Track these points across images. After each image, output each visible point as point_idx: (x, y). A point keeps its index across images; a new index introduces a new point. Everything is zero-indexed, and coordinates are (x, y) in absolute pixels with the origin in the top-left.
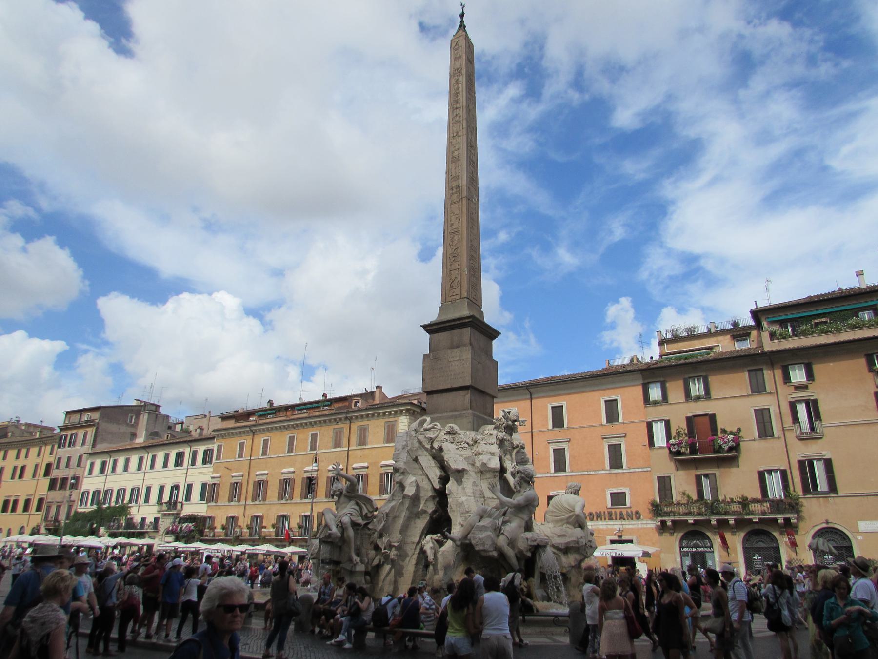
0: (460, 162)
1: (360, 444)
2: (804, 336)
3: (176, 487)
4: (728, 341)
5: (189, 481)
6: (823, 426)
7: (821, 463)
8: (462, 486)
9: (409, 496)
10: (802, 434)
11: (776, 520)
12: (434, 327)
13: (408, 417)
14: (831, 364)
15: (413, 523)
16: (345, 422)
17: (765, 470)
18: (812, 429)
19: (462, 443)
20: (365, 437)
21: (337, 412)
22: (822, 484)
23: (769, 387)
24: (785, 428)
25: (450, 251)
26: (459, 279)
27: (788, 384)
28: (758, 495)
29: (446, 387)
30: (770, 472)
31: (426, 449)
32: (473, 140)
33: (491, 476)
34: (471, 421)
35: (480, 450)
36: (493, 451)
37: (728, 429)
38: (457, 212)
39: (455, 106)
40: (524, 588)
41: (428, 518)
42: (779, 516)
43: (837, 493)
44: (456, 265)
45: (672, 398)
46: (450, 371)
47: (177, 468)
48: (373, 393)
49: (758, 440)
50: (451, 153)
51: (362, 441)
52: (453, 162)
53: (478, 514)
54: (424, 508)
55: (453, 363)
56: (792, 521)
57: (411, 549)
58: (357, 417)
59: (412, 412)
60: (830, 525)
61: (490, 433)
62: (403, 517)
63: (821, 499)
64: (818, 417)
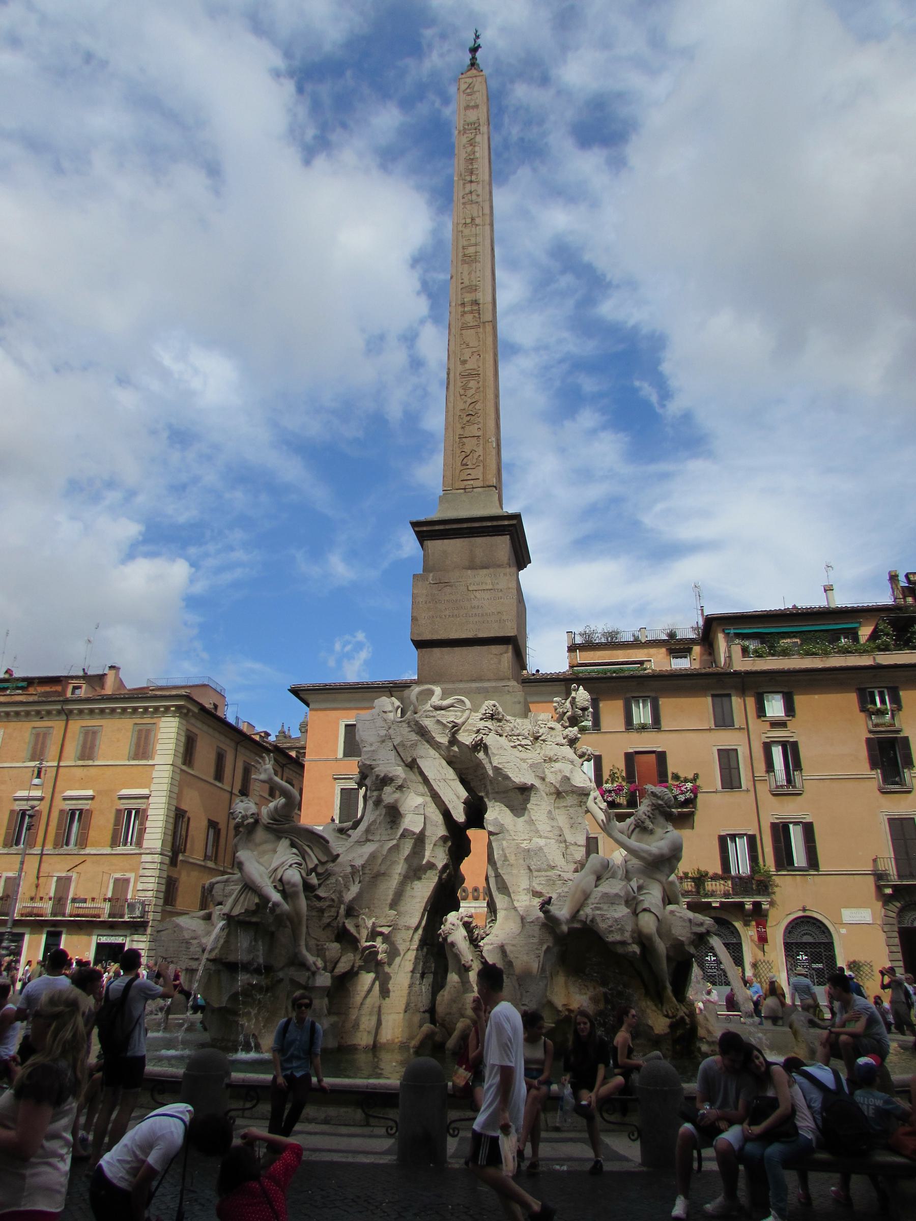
0: (478, 265)
1: (82, 758)
2: (785, 656)
4: (660, 656)
6: (804, 778)
7: (799, 828)
8: (526, 817)
9: (414, 834)
10: (777, 787)
11: (742, 904)
12: (437, 528)
13: (177, 719)
14: (816, 697)
15: (409, 888)
16: (57, 718)
17: (728, 834)
18: (789, 781)
19: (520, 738)
20: (92, 747)
21: (41, 699)
22: (799, 857)
23: (738, 720)
25: (461, 405)
27: (763, 719)
28: (719, 871)
30: (733, 837)
31: (436, 745)
33: (575, 802)
34: (522, 700)
35: (551, 754)
37: (682, 775)
39: (468, 178)
40: (686, 1017)
41: (436, 879)
42: (748, 900)
43: (818, 870)
44: (473, 430)
45: (605, 725)
48: (101, 678)
49: (721, 792)
50: (461, 249)
51: (87, 752)
52: (464, 262)
53: (595, 872)
54: (432, 860)
55: (477, 594)
56: (763, 906)
57: (404, 941)
58: (81, 711)
59: (185, 711)
60: (808, 913)
61: (550, 726)
62: (397, 877)
63: (798, 877)
64: (798, 766)
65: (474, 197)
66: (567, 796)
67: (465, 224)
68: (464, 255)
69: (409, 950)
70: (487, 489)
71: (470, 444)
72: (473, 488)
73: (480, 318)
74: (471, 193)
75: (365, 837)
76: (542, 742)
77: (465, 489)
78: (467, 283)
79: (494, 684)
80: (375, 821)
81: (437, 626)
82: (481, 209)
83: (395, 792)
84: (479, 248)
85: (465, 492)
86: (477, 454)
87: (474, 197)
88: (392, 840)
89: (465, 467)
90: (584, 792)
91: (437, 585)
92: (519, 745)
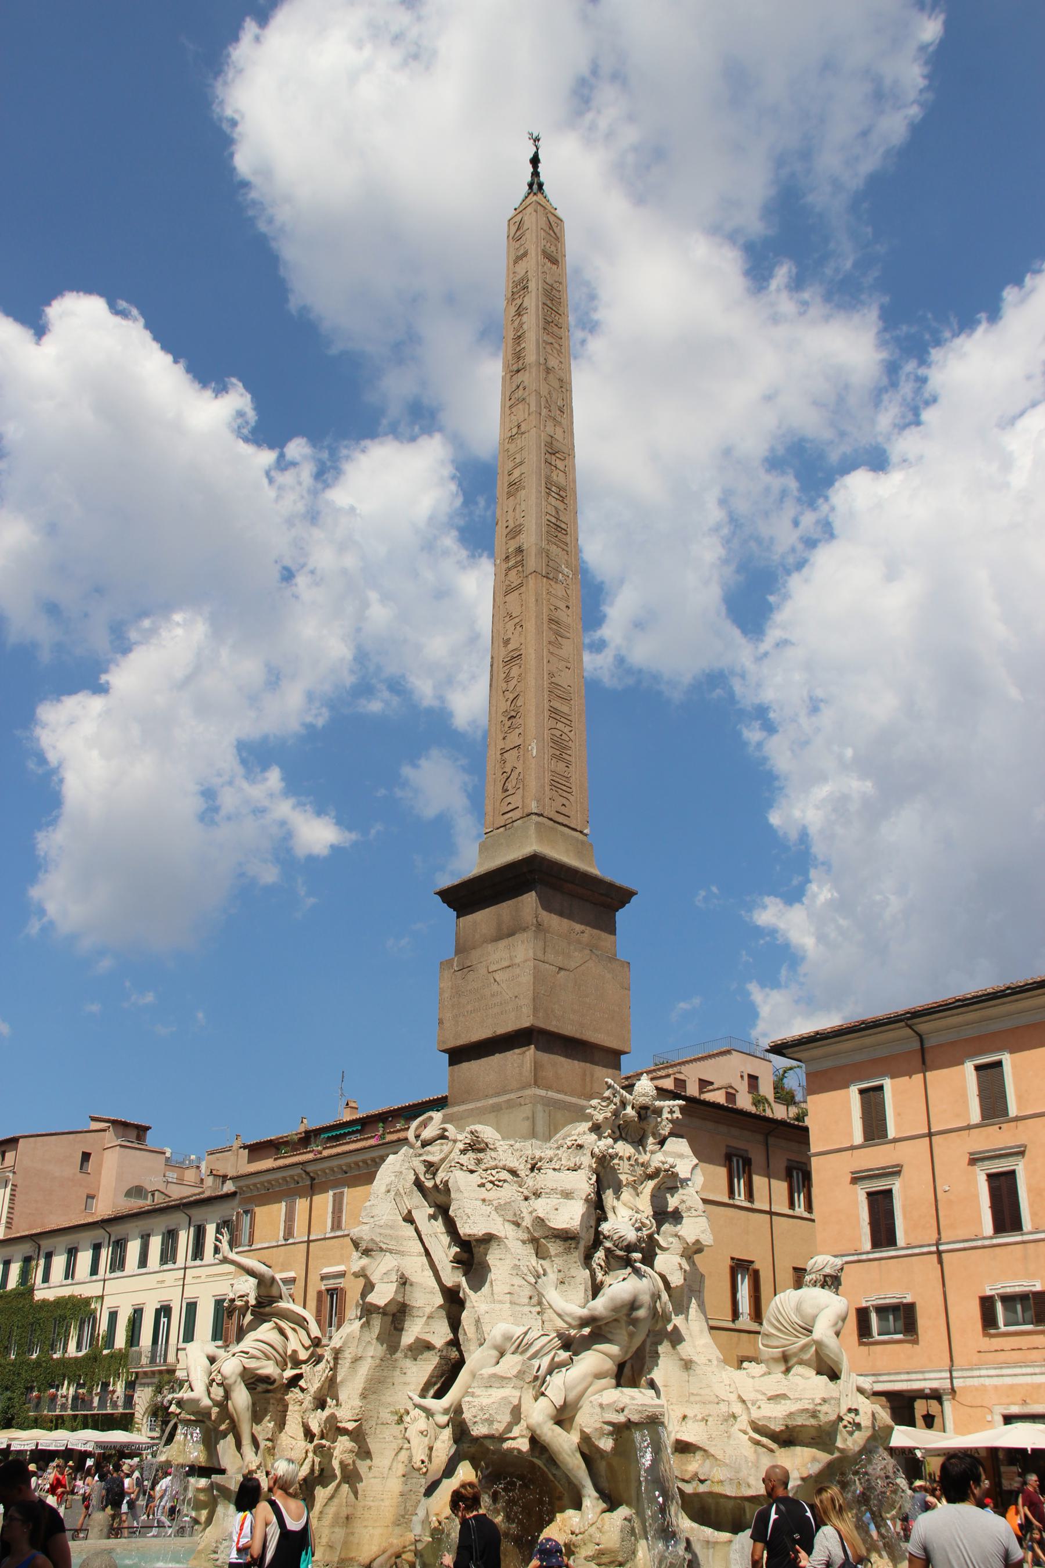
3: (164, 1311)
5: (190, 1293)
9: (379, 1307)
19: (494, 1172)
25: (504, 706)
32: (559, 435)
33: (561, 1250)
36: (568, 1187)
39: (515, 367)
44: (514, 739)
46: (493, 995)
47: (165, 1267)
65: (520, 392)
69: (401, 1449)
70: (526, 818)
77: (505, 826)
86: (517, 771)
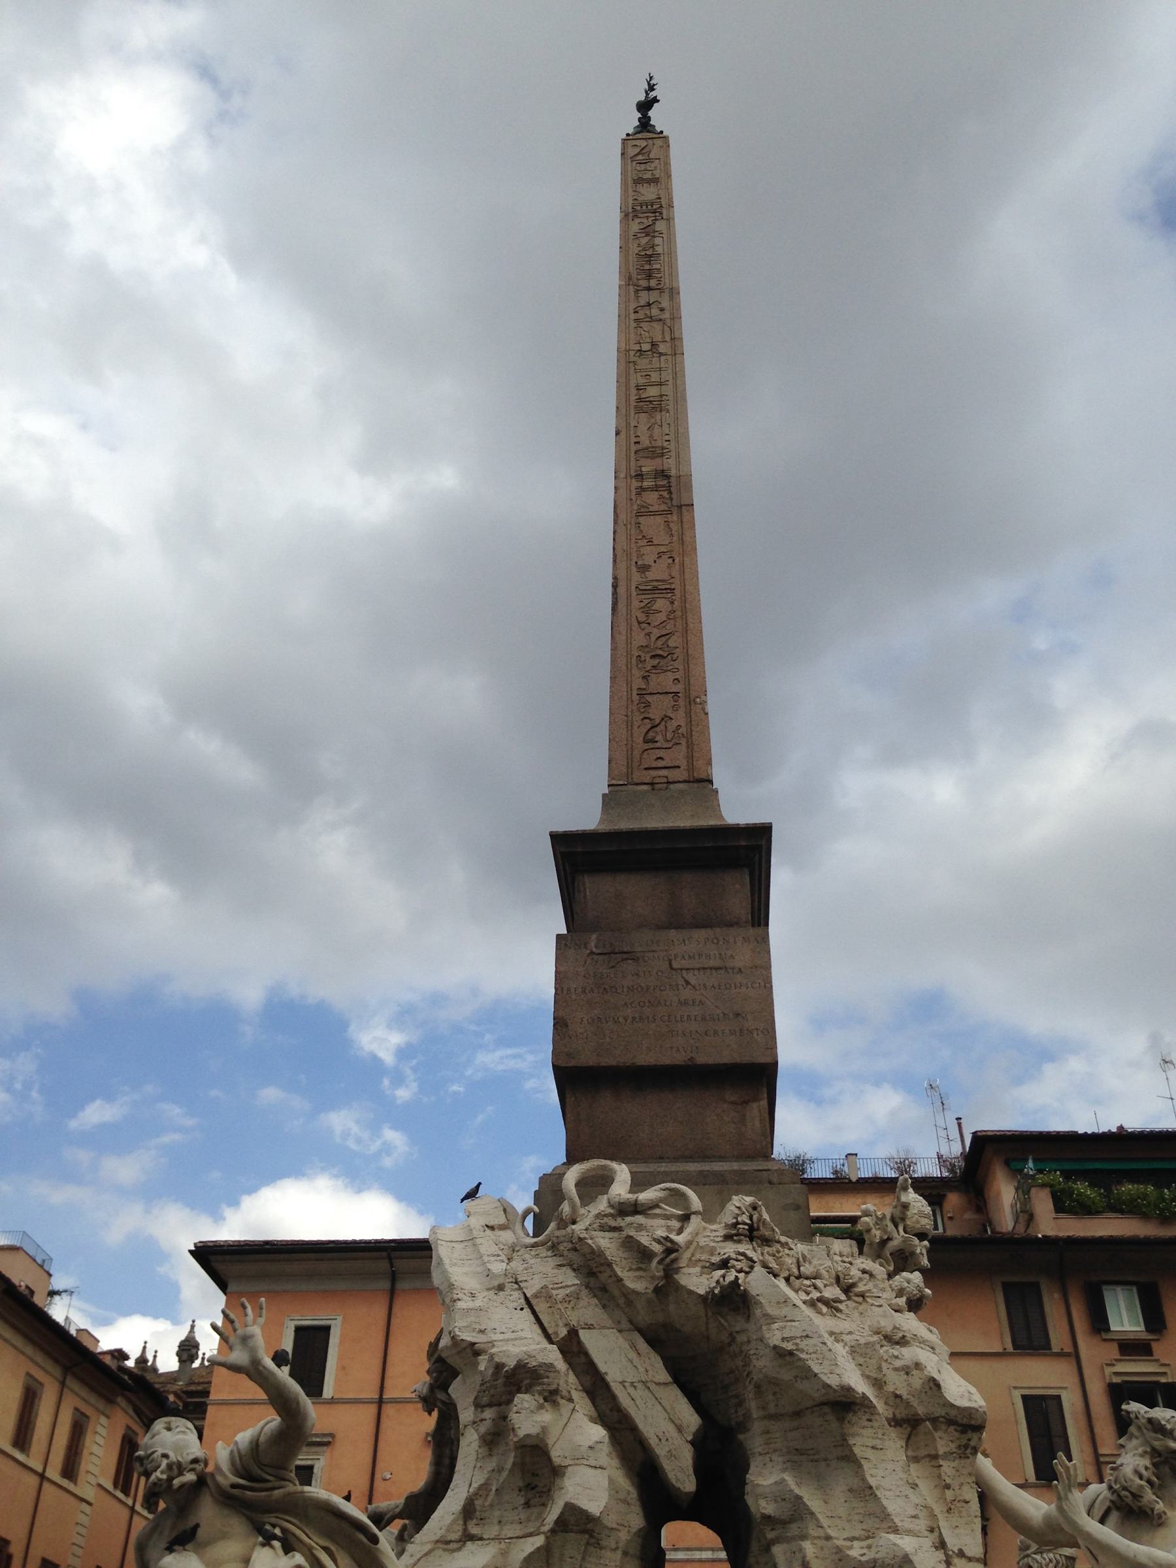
19: (818, 1282)
23: (1058, 1338)
24: (1102, 1459)
25: (639, 639)
26: (682, 723)
27: (1105, 1336)
29: (666, 1060)
33: (953, 1447)
38: (661, 538)
39: (644, 283)
44: (665, 681)
50: (633, 391)
52: (639, 410)
66: (936, 1430)
67: (640, 351)
68: (640, 400)
71: (659, 707)
72: (668, 783)
73: (671, 499)
74: (649, 305)
75: (461, 1528)
76: (860, 1299)
77: (652, 784)
78: (645, 442)
79: (736, 1166)
80: (485, 1487)
81: (608, 1039)
82: (666, 329)
83: (541, 1407)
84: (666, 390)
85: (653, 789)
86: (674, 724)
87: (655, 312)
88: (531, 1535)
89: (651, 745)
90: (973, 1422)
91: (606, 957)
92: (820, 1300)
